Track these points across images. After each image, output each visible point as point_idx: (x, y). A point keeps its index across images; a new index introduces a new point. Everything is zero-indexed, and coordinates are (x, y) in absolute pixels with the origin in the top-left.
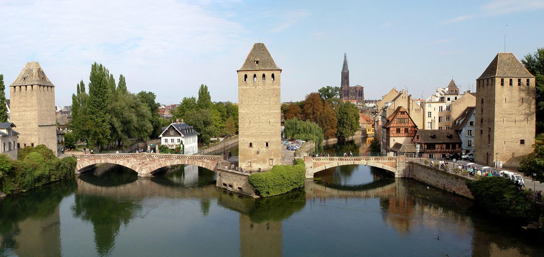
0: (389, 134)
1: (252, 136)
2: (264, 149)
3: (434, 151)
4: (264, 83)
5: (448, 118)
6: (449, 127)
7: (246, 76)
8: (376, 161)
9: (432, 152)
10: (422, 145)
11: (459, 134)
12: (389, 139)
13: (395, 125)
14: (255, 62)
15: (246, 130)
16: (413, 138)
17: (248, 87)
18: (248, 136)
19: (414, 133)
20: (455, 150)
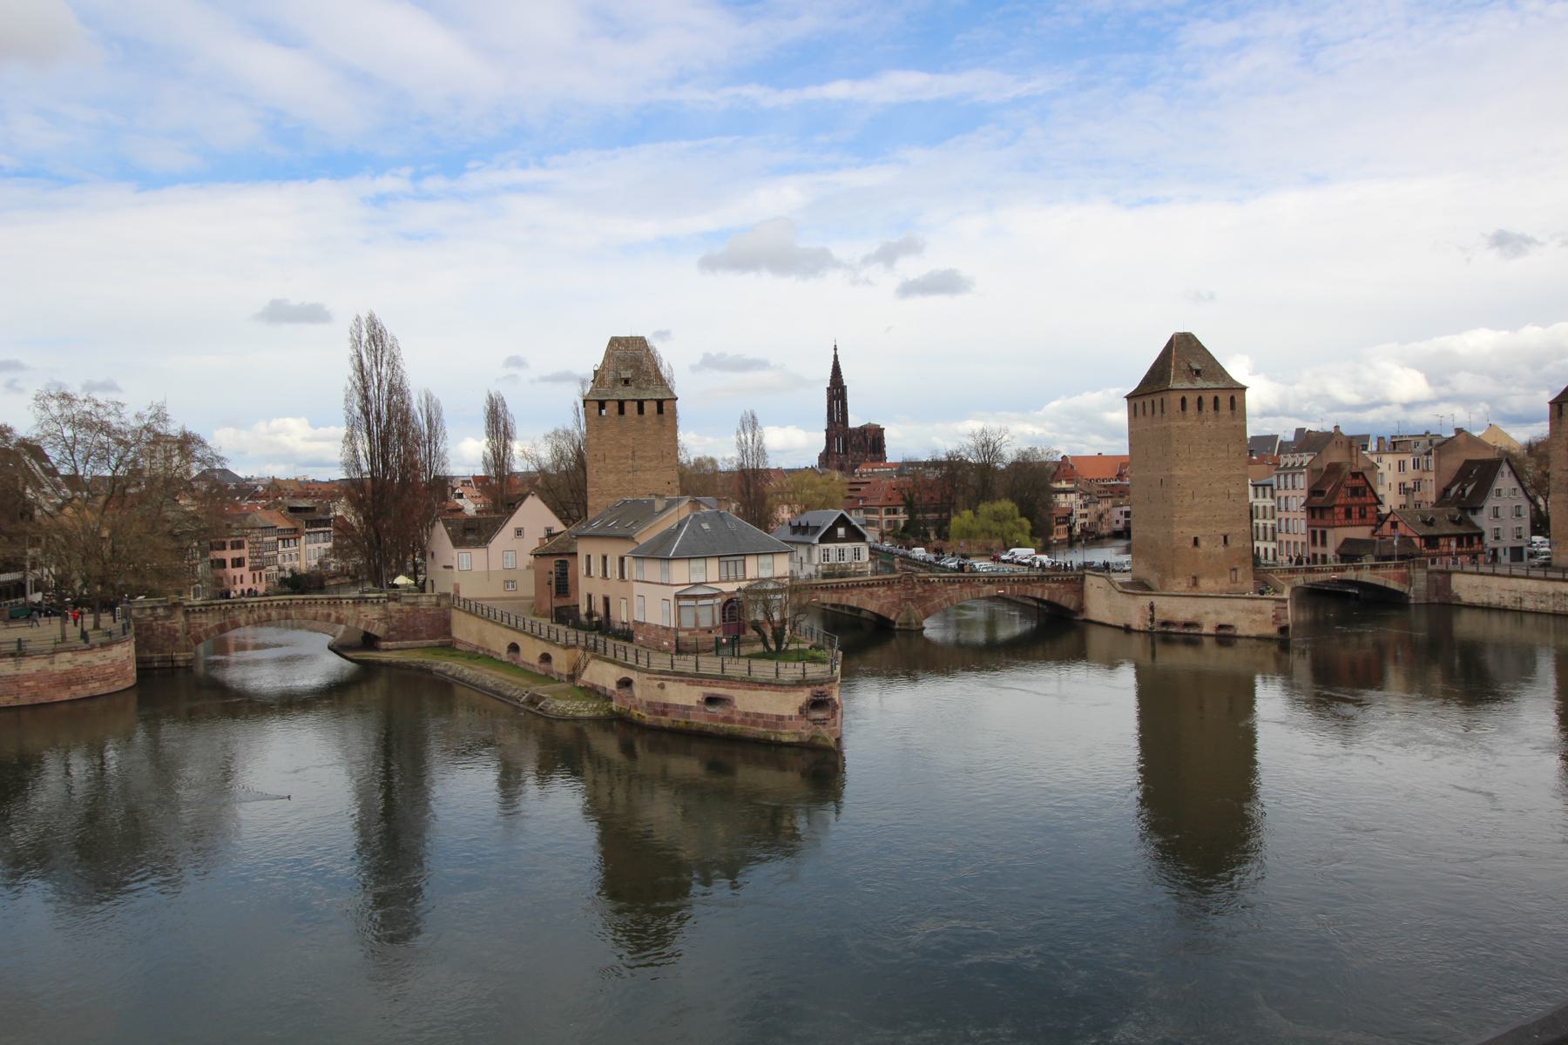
0: (1334, 520)
1: (1198, 524)
2: (1221, 549)
3: (1437, 551)
4: (1217, 416)
6: (1419, 505)
7: (1183, 400)
8: (1373, 572)
9: (1435, 555)
10: (1412, 541)
11: (1470, 516)
12: (1324, 534)
13: (1342, 502)
14: (1194, 373)
16: (1373, 528)
17: (1189, 423)
19: (1375, 516)
20: (1472, 549)
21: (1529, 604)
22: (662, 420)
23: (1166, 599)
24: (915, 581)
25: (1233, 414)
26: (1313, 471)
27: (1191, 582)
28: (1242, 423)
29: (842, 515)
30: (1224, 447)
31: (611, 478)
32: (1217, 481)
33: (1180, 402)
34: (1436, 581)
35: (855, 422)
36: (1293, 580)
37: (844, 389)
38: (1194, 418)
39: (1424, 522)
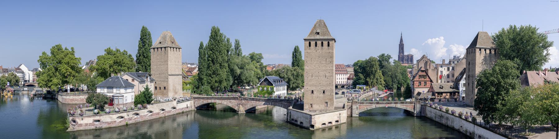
2: (322, 95)
4: (322, 49)
5: (453, 76)
7: (310, 43)
8: (402, 104)
13: (418, 80)
15: (309, 81)
17: (311, 51)
18: (310, 86)
21: (437, 120)
22: (165, 53)
23: (293, 111)
24: (242, 98)
25: (328, 48)
26: (415, 70)
27: (310, 106)
28: (332, 51)
29: (266, 78)
30: (325, 60)
31: (155, 67)
32: (321, 71)
33: (308, 44)
34: (424, 108)
35: (406, 53)
36: (371, 106)
37: (403, 44)
38: (313, 49)
39: (440, 88)
